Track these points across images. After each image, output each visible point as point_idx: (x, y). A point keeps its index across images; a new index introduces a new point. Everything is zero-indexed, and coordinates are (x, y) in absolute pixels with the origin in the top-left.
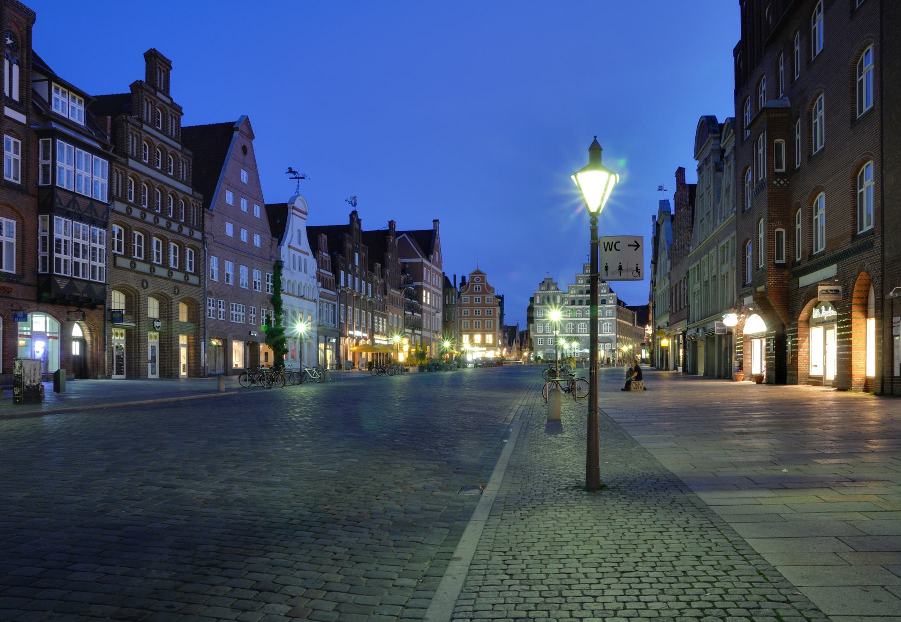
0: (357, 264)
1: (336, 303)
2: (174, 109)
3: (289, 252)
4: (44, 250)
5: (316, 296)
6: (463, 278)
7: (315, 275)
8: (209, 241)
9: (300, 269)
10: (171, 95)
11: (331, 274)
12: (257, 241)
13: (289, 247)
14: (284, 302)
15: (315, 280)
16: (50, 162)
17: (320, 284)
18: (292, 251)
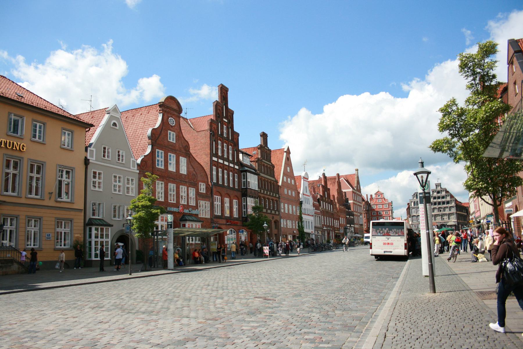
0: (326, 197)
1: (320, 216)
2: (269, 151)
3: (303, 197)
4: (244, 209)
5: (313, 214)
6: (371, 196)
7: (312, 205)
8: (281, 197)
9: (307, 203)
10: (268, 146)
11: (317, 203)
12: (286, 190)
13: (303, 194)
14: (303, 218)
15: (313, 207)
16: (245, 180)
17: (314, 208)
18: (305, 196)
